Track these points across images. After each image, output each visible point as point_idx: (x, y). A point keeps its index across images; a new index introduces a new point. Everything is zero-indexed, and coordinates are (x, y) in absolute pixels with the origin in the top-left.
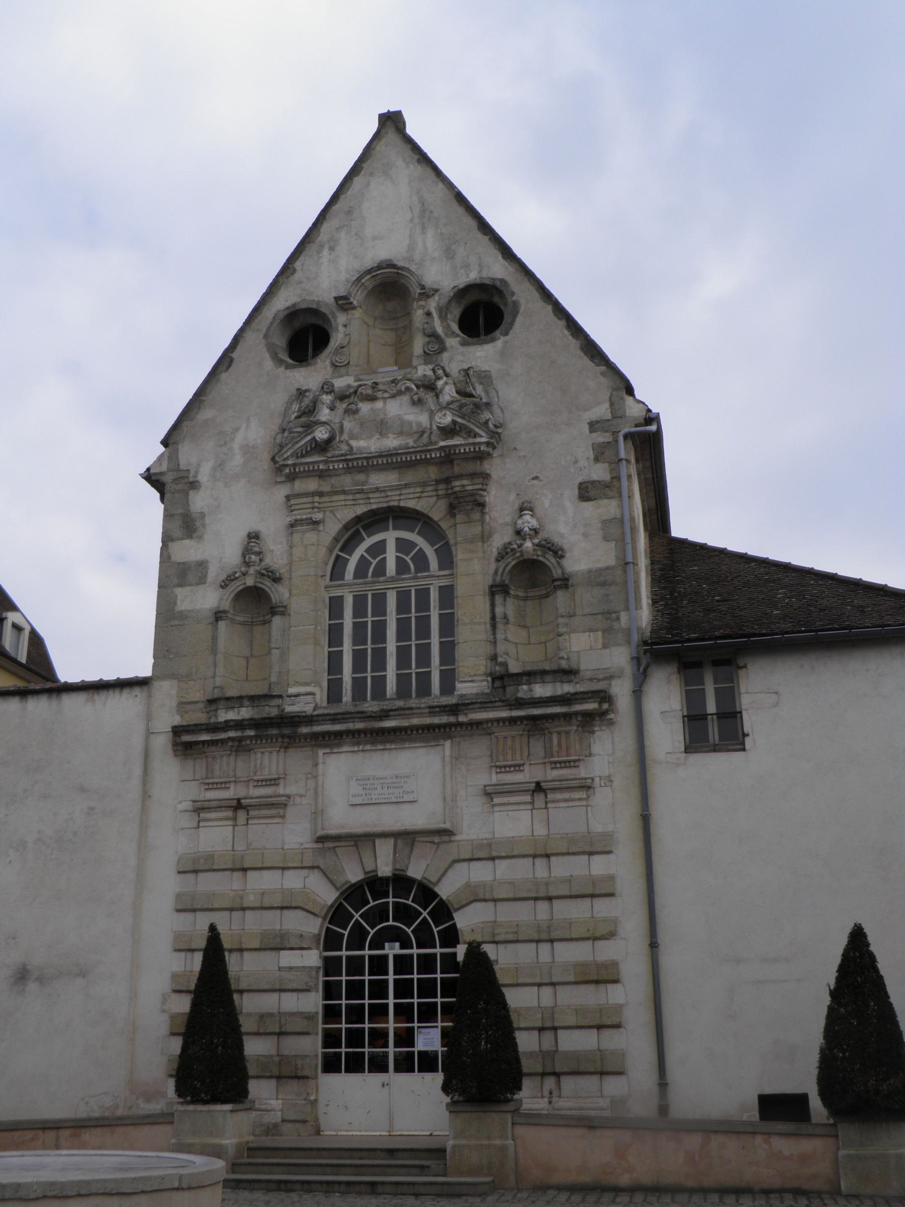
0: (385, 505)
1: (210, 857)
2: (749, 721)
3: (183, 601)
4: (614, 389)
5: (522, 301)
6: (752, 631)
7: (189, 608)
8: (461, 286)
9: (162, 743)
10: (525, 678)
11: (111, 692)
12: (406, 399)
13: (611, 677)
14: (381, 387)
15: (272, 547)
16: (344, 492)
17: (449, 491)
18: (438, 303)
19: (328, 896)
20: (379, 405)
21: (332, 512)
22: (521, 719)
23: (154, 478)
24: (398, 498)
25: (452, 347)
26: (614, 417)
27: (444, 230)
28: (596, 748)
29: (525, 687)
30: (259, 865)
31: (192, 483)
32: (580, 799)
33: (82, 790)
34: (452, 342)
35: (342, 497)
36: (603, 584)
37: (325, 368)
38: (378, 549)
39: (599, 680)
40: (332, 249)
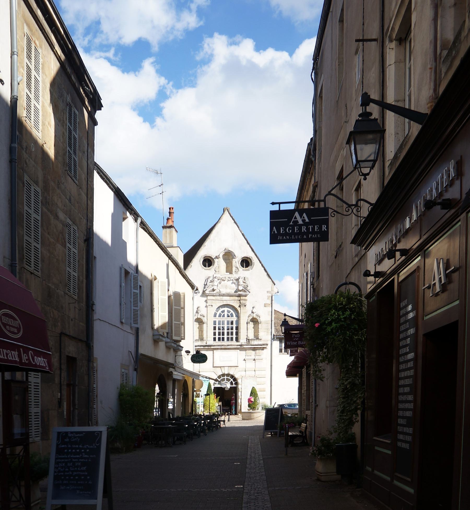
14: (226, 278)
26: (272, 291)
34: (241, 269)
36: (267, 323)
38: (223, 312)
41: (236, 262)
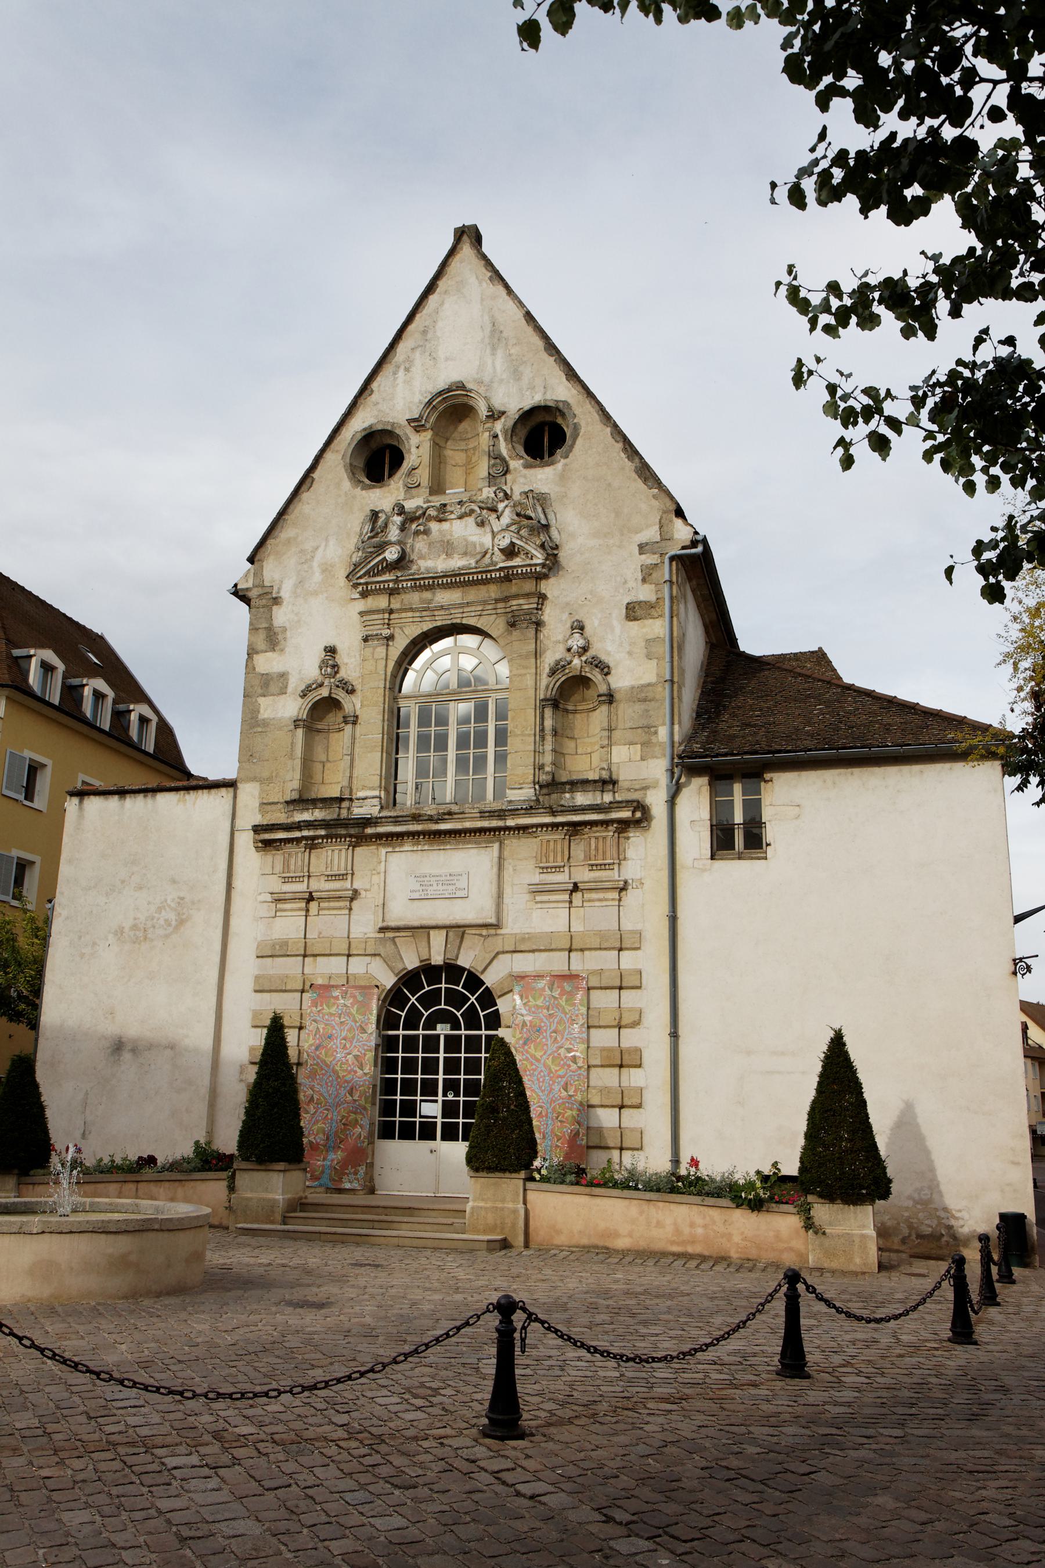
0: (449, 622)
1: (284, 943)
2: (771, 833)
3: (266, 710)
4: (664, 512)
5: (583, 424)
6: (778, 747)
7: (272, 716)
8: (526, 408)
9: (245, 840)
10: (568, 787)
11: (200, 792)
12: (470, 521)
13: (645, 788)
14: (449, 508)
15: (346, 661)
16: (411, 610)
17: (508, 610)
18: (504, 425)
19: (388, 981)
20: (445, 525)
21: (401, 628)
22: (563, 824)
23: (240, 593)
24: (460, 615)
25: (515, 469)
27: (512, 351)
28: (630, 853)
29: (567, 795)
30: (328, 952)
31: (275, 599)
32: (613, 899)
33: (174, 881)
35: (410, 614)
36: (645, 700)
37: (398, 489)
39: (636, 790)
40: (407, 370)
41: (496, 436)
